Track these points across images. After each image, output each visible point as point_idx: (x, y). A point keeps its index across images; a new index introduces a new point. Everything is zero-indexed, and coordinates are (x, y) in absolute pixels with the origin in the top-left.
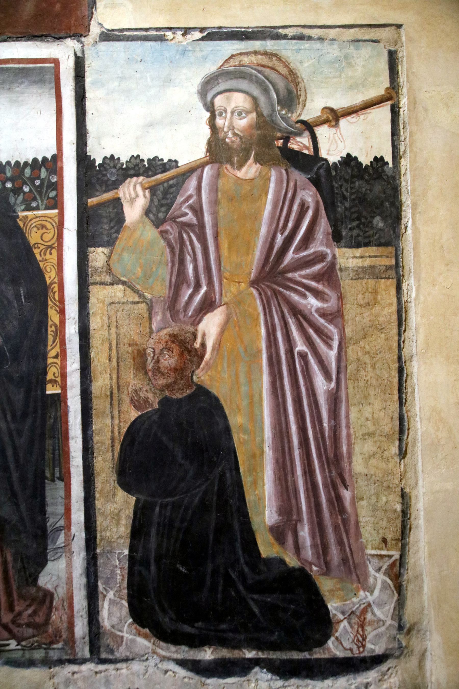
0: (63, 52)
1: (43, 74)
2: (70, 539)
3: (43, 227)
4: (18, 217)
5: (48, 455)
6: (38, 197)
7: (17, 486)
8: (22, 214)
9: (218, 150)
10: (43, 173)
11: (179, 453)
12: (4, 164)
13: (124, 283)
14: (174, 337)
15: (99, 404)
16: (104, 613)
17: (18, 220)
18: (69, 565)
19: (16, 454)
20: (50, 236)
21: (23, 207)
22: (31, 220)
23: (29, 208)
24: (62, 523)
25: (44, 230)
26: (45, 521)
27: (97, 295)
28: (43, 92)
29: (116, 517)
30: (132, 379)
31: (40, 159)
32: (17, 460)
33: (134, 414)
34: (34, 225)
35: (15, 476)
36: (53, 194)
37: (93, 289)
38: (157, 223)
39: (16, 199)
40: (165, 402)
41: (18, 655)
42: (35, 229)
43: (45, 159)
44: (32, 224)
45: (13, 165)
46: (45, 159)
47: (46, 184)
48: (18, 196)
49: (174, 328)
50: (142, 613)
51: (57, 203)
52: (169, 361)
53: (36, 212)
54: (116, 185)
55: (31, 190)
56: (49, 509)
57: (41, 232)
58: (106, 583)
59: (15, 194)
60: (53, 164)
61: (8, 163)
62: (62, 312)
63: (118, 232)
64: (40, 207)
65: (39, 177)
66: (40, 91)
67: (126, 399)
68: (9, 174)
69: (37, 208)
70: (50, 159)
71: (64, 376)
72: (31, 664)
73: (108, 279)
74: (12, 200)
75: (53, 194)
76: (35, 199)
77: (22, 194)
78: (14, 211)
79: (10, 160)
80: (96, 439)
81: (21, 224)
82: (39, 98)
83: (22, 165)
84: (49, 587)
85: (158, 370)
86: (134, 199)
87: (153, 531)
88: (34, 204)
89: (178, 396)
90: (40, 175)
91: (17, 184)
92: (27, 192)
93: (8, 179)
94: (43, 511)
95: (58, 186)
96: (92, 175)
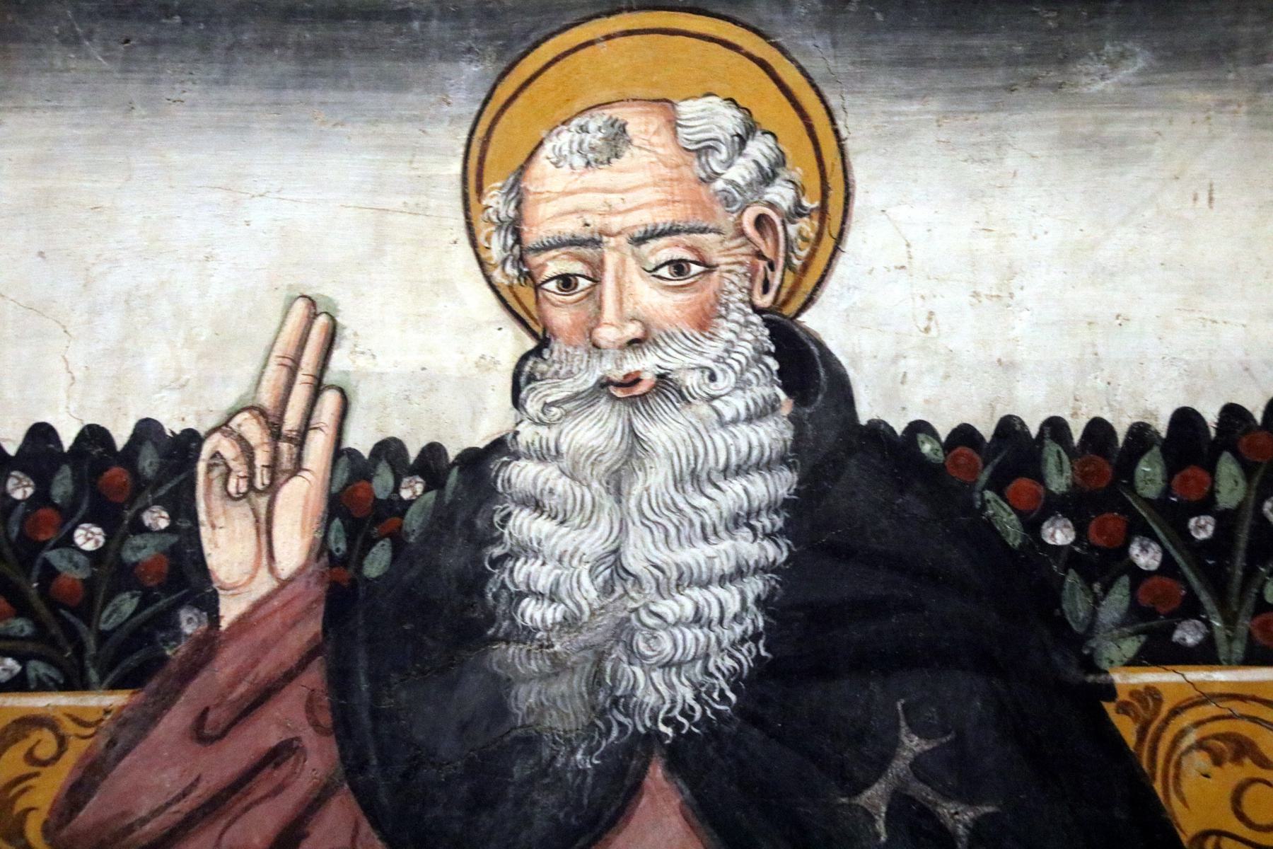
3: (1242, 749)
4: (1109, 691)
6: (1204, 597)
8: (1128, 679)
10: (1230, 486)
12: (1034, 431)
17: (1110, 707)
21: (1131, 646)
22: (1175, 712)
23: (1160, 652)
25: (1250, 768)
28: (1224, 104)
31: (1211, 415)
34: (1191, 738)
39: (1097, 601)
42: (1200, 760)
43: (1233, 413)
44: (1183, 733)
45: (1077, 437)
46: (1233, 413)
47: (1243, 537)
48: (1106, 590)
53: (1197, 675)
55: (1167, 560)
57: (1235, 773)
59: (1088, 580)
61: (1055, 427)
64: (1223, 650)
65: (1206, 505)
66: (1206, 97)
68: (1058, 482)
69: (1205, 655)
70: (1259, 417)
74: (1076, 603)
76: (1191, 609)
77: (1125, 580)
78: (1090, 665)
79: (1065, 414)
81: (1127, 729)
82: (1203, 130)
83: (1121, 438)
88: (1189, 634)
90: (1212, 493)
91: (1100, 532)
92: (1149, 574)
93: (1054, 506)
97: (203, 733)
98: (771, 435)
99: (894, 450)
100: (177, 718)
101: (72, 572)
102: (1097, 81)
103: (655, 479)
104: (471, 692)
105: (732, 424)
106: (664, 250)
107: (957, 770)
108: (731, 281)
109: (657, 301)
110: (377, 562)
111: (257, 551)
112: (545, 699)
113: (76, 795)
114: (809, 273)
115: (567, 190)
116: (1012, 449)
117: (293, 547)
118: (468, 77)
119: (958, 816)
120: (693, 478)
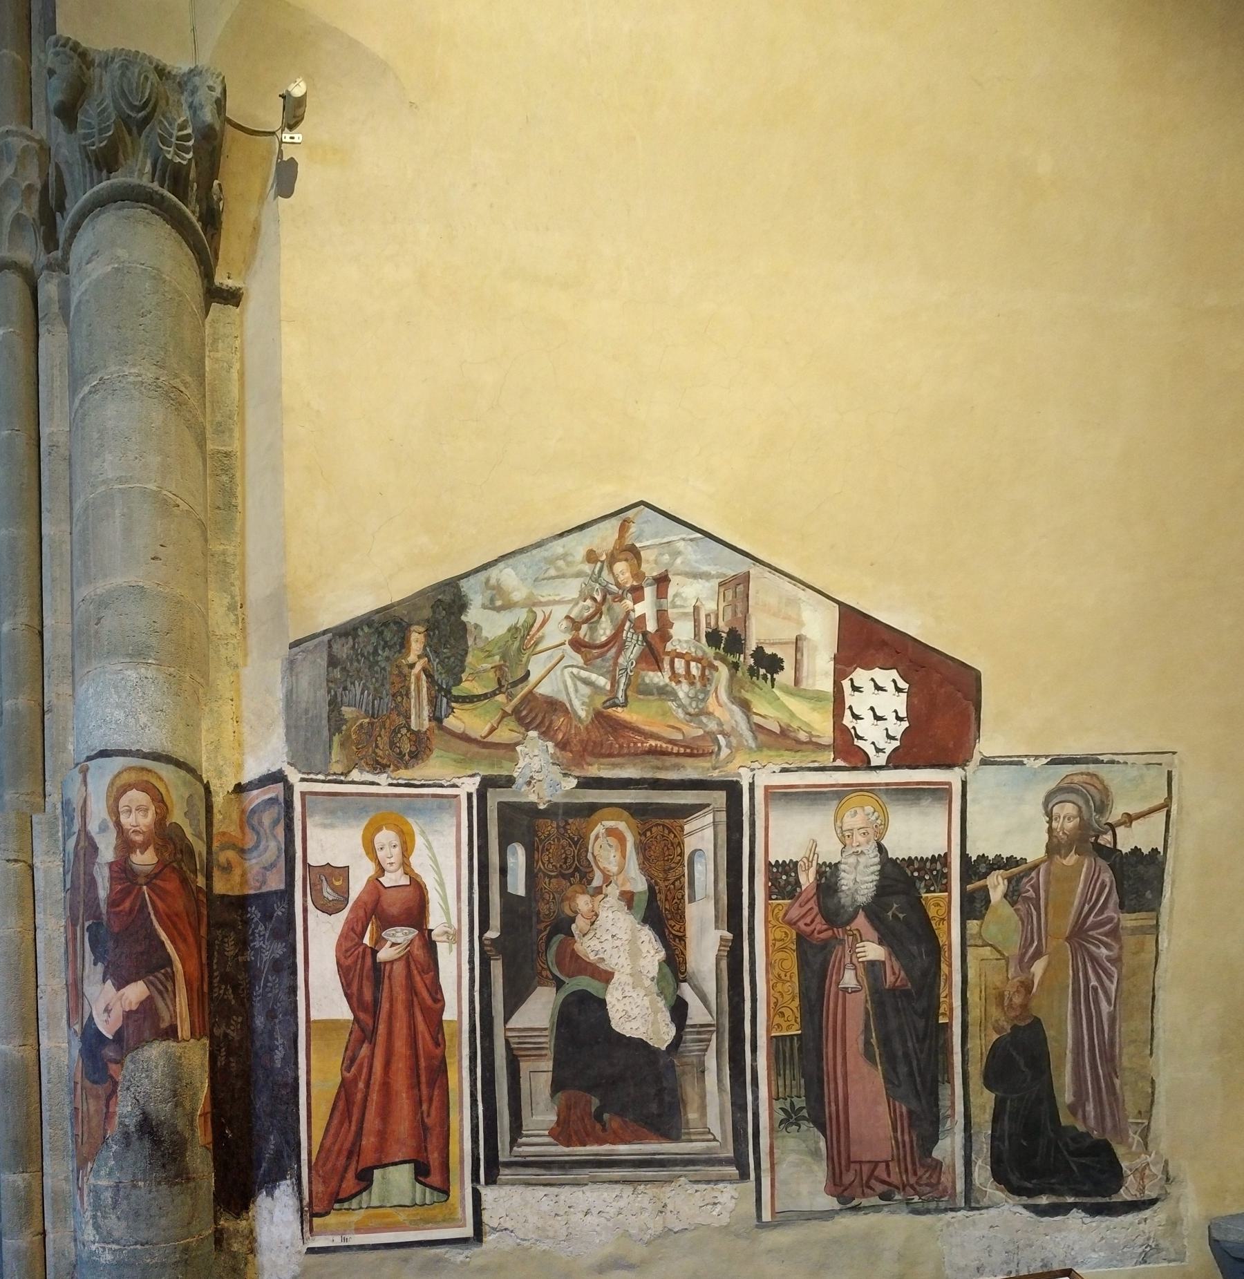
0: (953, 777)
1: (940, 793)
2: (954, 1123)
3: (939, 905)
5: (940, 1066)
7: (919, 1087)
9: (1053, 848)
10: (939, 866)
11: (1022, 1063)
13: (991, 945)
14: (1022, 982)
15: (973, 1030)
16: (976, 1175)
18: (953, 1142)
19: (918, 1065)
20: (943, 911)
23: (928, 891)
24: (949, 1112)
26: (938, 1112)
27: (971, 952)
29: (983, 1108)
30: (995, 1012)
32: (919, 1069)
33: (995, 1037)
35: (918, 1080)
36: (944, 881)
37: (970, 951)
38: (1013, 904)
40: (1014, 1028)
41: (919, 1206)
49: (1022, 977)
50: (999, 1175)
51: (947, 888)
52: (1017, 1000)
54: (985, 876)
56: (940, 1103)
58: (977, 1154)
60: (944, 859)
62: (950, 966)
63: (987, 909)
67: (990, 1026)
71: (951, 1010)
72: (928, 1212)
73: (980, 942)
74: (918, 885)
75: (944, 881)
80: (971, 1053)
84: (940, 1158)
85: (1010, 1006)
86: (997, 885)
87: (1006, 1118)
89: (1023, 1024)
94: (938, 1106)
95: (947, 876)
96: (974, 869)
97: (801, 906)
98: (877, 860)
99: (894, 862)
100: (797, 904)
101: (782, 883)
102: (924, 803)
103: (861, 867)
104: (835, 901)
105: (871, 859)
106: (862, 831)
107: (901, 909)
108: (871, 835)
109: (861, 839)
110: (823, 880)
111: (807, 879)
112: (845, 900)
113: (785, 915)
114: (882, 835)
115: (850, 821)
116: (910, 861)
117: (812, 879)
118: (835, 802)
119: (901, 916)
120: (866, 867)
